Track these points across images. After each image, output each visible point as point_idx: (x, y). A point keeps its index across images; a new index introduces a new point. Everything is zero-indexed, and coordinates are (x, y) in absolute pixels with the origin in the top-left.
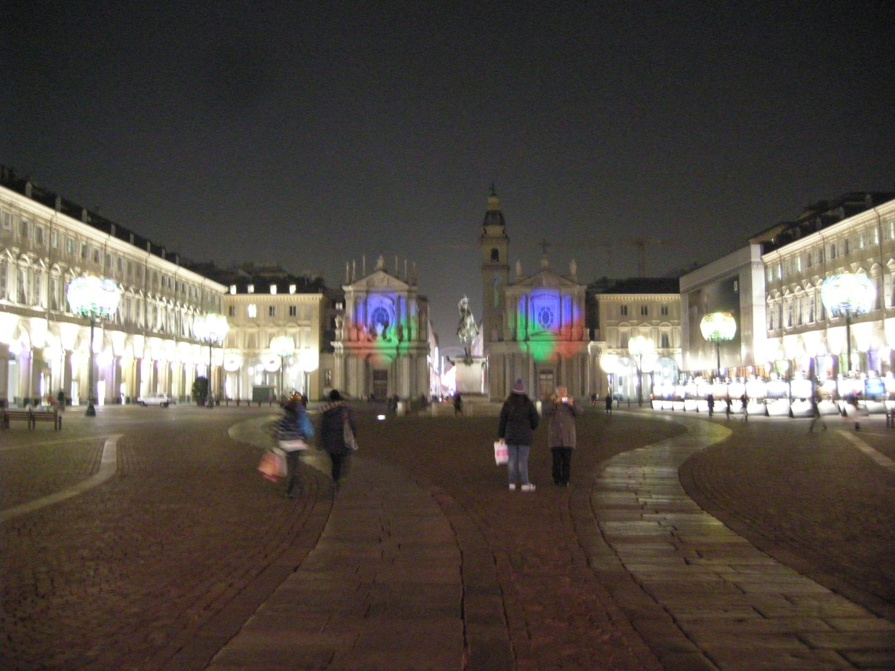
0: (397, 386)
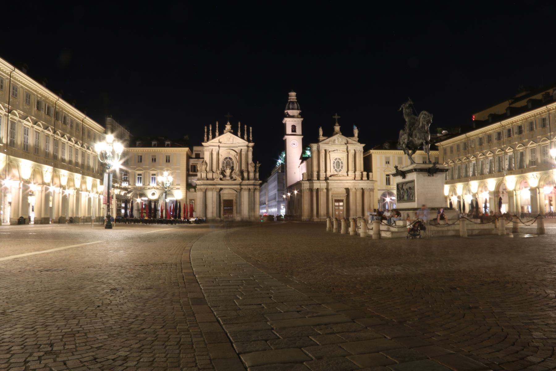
0: (239, 212)
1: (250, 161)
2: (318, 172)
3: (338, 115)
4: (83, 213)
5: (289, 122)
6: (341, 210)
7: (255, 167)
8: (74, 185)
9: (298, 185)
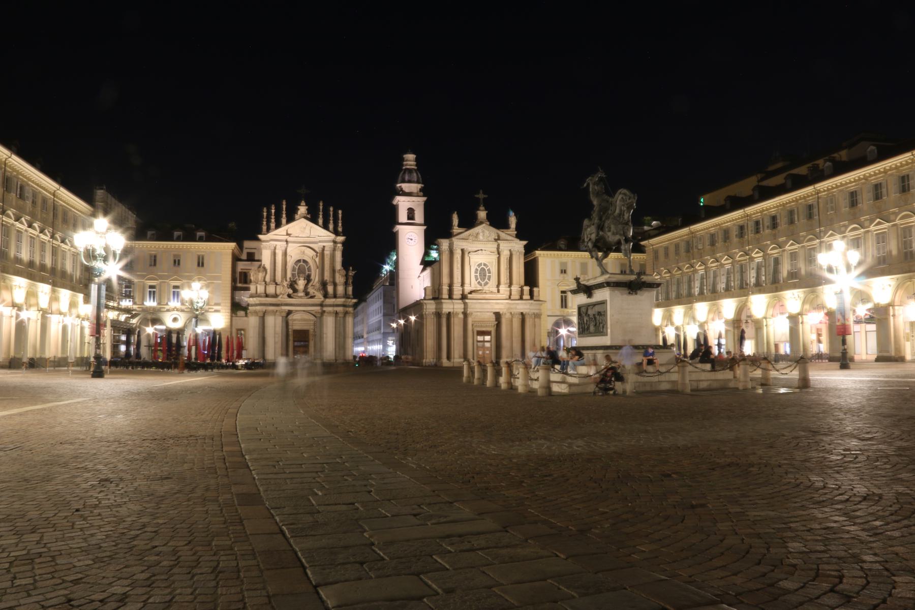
0: (320, 349)
1: (338, 265)
2: (451, 286)
3: (484, 193)
4: (52, 350)
5: (403, 204)
6: (487, 348)
7: (347, 276)
8: (37, 304)
9: (417, 306)
